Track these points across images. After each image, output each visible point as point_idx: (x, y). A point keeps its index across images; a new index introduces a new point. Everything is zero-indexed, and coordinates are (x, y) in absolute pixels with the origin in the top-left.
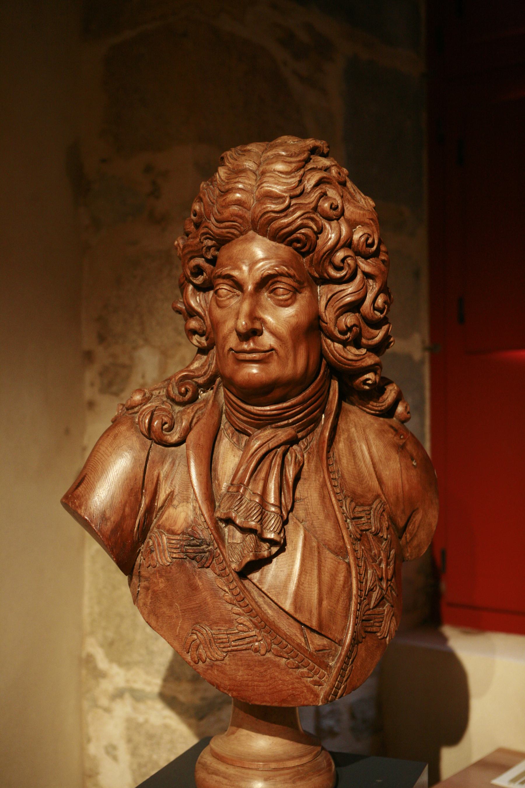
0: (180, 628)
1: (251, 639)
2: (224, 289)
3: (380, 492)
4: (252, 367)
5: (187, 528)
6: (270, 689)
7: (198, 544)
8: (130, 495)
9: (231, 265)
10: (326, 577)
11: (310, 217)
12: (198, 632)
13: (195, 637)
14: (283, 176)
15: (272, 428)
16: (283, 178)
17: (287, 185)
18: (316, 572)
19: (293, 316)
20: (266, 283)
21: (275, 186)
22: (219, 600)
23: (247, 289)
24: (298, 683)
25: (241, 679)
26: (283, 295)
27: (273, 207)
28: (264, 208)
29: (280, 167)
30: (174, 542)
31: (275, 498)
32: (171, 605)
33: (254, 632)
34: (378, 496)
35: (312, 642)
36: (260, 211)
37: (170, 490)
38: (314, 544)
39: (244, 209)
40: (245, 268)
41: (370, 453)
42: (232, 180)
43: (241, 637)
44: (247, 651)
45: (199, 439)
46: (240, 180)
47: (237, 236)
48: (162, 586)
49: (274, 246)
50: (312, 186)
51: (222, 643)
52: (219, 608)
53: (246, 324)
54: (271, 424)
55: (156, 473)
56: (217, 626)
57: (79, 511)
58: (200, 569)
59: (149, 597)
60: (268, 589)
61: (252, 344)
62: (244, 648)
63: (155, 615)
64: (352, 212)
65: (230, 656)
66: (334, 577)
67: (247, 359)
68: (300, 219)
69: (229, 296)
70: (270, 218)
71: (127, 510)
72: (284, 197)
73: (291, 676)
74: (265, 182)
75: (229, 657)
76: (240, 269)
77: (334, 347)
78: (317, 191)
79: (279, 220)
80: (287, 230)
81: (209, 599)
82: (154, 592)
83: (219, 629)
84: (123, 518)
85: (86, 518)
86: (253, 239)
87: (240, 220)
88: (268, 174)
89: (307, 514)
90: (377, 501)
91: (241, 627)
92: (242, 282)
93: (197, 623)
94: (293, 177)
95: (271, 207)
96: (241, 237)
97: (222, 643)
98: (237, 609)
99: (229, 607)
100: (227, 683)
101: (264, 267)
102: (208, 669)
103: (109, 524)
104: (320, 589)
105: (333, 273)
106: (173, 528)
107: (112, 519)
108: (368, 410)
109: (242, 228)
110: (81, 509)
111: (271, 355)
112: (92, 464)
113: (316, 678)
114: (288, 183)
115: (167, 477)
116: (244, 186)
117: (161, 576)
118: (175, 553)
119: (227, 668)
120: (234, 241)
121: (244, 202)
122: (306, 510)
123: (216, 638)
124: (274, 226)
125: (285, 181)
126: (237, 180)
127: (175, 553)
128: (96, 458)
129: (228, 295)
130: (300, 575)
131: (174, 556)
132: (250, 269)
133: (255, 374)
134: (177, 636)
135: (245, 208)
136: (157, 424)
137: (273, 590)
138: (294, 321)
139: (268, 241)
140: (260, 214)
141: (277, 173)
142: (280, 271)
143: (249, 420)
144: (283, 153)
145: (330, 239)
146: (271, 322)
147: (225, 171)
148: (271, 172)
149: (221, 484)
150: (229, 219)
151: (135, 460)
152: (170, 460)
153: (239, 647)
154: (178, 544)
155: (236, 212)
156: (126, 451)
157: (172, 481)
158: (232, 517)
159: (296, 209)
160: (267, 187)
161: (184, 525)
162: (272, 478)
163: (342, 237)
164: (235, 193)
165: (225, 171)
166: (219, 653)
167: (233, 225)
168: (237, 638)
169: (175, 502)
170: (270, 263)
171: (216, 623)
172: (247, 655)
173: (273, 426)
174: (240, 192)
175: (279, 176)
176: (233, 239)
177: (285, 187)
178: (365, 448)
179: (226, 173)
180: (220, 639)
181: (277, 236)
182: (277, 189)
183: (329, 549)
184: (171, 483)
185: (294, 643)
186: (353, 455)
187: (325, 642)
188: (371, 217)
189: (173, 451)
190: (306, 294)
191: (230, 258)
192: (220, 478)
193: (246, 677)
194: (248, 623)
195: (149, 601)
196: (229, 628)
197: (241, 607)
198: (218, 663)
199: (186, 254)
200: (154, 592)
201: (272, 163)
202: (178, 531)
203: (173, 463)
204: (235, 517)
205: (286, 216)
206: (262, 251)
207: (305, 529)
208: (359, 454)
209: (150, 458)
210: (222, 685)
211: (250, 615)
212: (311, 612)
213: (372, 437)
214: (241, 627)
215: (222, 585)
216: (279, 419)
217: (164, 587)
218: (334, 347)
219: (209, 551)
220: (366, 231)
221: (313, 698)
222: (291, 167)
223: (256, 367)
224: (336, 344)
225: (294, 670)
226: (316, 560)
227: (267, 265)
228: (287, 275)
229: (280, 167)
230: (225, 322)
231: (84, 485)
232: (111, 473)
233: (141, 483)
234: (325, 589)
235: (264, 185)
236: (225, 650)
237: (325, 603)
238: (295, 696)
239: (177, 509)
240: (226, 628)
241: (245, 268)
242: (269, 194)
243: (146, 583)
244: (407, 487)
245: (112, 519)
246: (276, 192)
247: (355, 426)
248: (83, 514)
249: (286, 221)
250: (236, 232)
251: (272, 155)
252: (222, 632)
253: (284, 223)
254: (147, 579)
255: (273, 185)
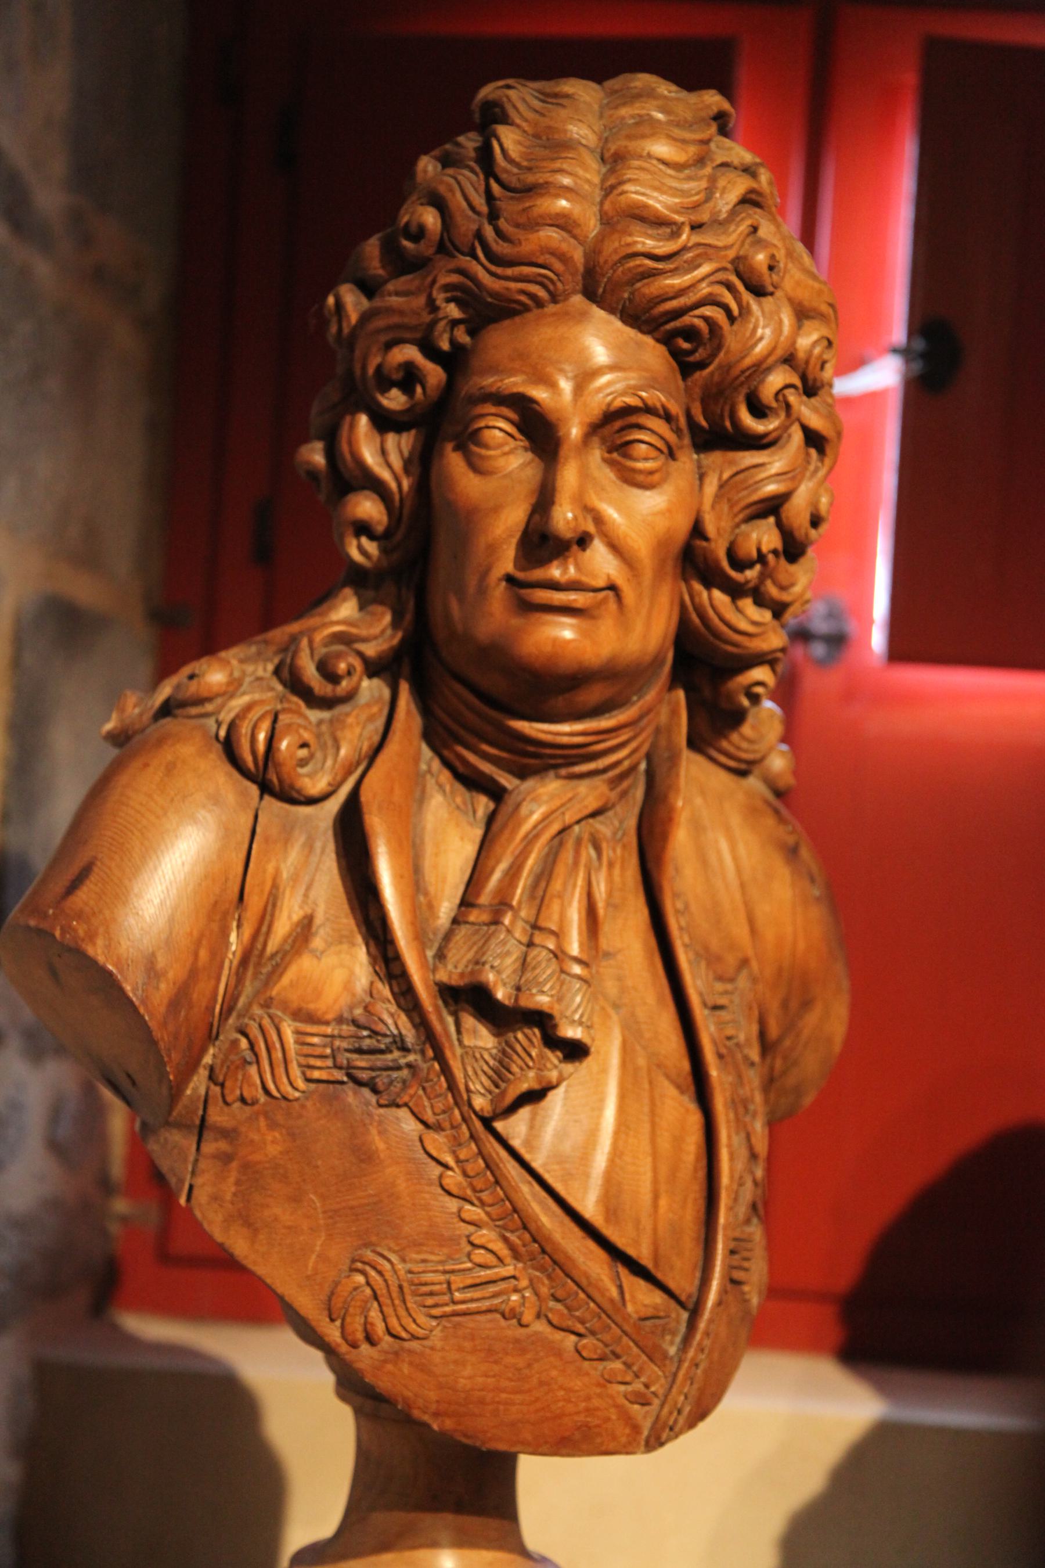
0: (318, 1256)
1: (502, 1286)
2: (498, 429)
3: (750, 953)
4: (563, 626)
5: (351, 1008)
6: (537, 1411)
7: (383, 1046)
8: (210, 918)
9: (524, 372)
10: (665, 1144)
11: (728, 280)
12: (368, 1268)
13: (360, 1279)
14: (670, 172)
15: (558, 777)
16: (671, 176)
17: (682, 196)
18: (646, 1127)
19: (661, 513)
20: (615, 427)
21: (655, 194)
22: (427, 1188)
23: (569, 433)
24: (600, 1396)
25: (468, 1387)
26: (646, 459)
27: (648, 244)
28: (629, 245)
29: (662, 149)
30: (316, 1040)
31: (581, 945)
32: (296, 1199)
33: (511, 1268)
34: (745, 962)
35: (633, 1297)
36: (615, 251)
37: (301, 913)
38: (641, 1062)
39: (572, 240)
40: (566, 386)
41: (735, 859)
42: (545, 164)
43: (478, 1281)
44: (489, 1316)
45: (392, 790)
46: (565, 166)
47: (539, 303)
48: (273, 1150)
49: (632, 339)
50: (730, 207)
51: (431, 1294)
52: (427, 1208)
53: (575, 518)
54: (555, 767)
55: (270, 868)
56: (418, 1253)
57: (90, 951)
58: (382, 1111)
59: (232, 1180)
60: (544, 1165)
61: (572, 570)
62: (484, 1308)
63: (247, 1223)
64: (798, 283)
65: (445, 1327)
66: (678, 1141)
67: (556, 603)
68: (707, 281)
69: (506, 449)
70: (641, 269)
71: (203, 954)
72: (675, 223)
73: (586, 1379)
74: (630, 180)
75: (442, 1331)
76: (553, 385)
77: (710, 598)
78: (743, 219)
79: (661, 278)
80: (674, 304)
81: (402, 1185)
82: (246, 1166)
83: (424, 1261)
84: (193, 974)
85: (110, 967)
86: (582, 316)
87: (558, 266)
88: (636, 163)
89: (623, 990)
90: (745, 973)
91: (480, 1256)
92: (553, 417)
93: (366, 1245)
94: (689, 178)
95: (644, 243)
96: (551, 308)
97: (431, 1294)
98: (473, 1212)
99: (453, 1205)
100: (433, 1395)
101: (611, 388)
102: (385, 1361)
103: (163, 986)
104: (655, 1170)
105: (747, 420)
106: (312, 1006)
107: (171, 975)
108: (723, 759)
109: (559, 285)
110: (94, 944)
111: (605, 600)
112: (109, 833)
113: (638, 1386)
114: (682, 191)
115: (295, 878)
116: (576, 184)
117: (273, 1125)
118: (319, 1068)
119: (437, 1358)
120: (529, 316)
121: (575, 222)
122: (620, 979)
123: (416, 1281)
124: (646, 291)
125: (675, 184)
126: (557, 165)
127: (319, 1068)
128: (119, 820)
129: (506, 444)
130: (617, 1133)
131: (316, 1074)
132: (579, 389)
133: (569, 642)
134: (308, 1277)
135: (575, 237)
136: (288, 746)
137: (556, 1167)
138: (662, 525)
139: (619, 324)
140: (616, 258)
141: (655, 162)
142: (650, 403)
143: (504, 755)
144: (660, 116)
145: (761, 339)
146: (614, 520)
147: (517, 137)
148: (640, 157)
149: (435, 904)
150: (534, 260)
151: (227, 832)
152: (302, 839)
153: (473, 1306)
154: (325, 1046)
155: (554, 244)
156: (204, 807)
157: (308, 888)
158: (488, 982)
159: (698, 256)
160: (636, 193)
161: (344, 1001)
162: (573, 894)
163: (782, 339)
164: (558, 196)
165: (517, 137)
166: (422, 1319)
167: (540, 275)
168: (469, 1282)
169: (317, 943)
170: (626, 379)
171: (417, 1245)
172: (488, 1326)
173: (563, 772)
174: (568, 195)
175: (660, 170)
176: (527, 309)
177: (677, 200)
178: (724, 846)
179: (520, 143)
180: (426, 1284)
181: (640, 316)
182: (659, 202)
183: (668, 1077)
184: (306, 895)
185: (603, 1295)
186: (704, 861)
187: (657, 1298)
188: (830, 301)
189: (308, 818)
190: (684, 463)
191: (522, 356)
192: (432, 890)
193: (480, 1380)
194: (499, 1247)
195: (229, 1189)
196: (450, 1257)
197: (483, 1204)
198: (414, 1345)
199: (378, 331)
200: (246, 1166)
201: (643, 136)
202: (325, 1013)
203: (309, 846)
204: (495, 984)
205: (674, 272)
206: (606, 347)
207: (625, 1027)
208: (713, 859)
209: (258, 830)
210: (420, 1402)
211: (504, 1227)
212: (637, 1222)
213: (735, 820)
214: (480, 1256)
215: (439, 1150)
216: (575, 756)
217: (281, 1153)
218: (710, 598)
219: (409, 1066)
220: (825, 331)
221: (628, 1435)
222: (686, 152)
223: (572, 626)
224: (717, 594)
225: (595, 1363)
226: (646, 1101)
227: (619, 381)
228: (661, 412)
229: (662, 149)
230: (497, 509)
231: (92, 886)
232: (167, 859)
233: (236, 889)
234: (664, 1170)
235: (629, 187)
236: (436, 1312)
237: (663, 1202)
238: (590, 1428)
239: (324, 960)
240: (442, 1258)
241: (566, 386)
242: (637, 211)
243: (223, 1145)
244: (801, 945)
245: (171, 975)
246: (657, 210)
247: (703, 793)
248: (101, 959)
249: (676, 282)
250: (542, 293)
251: (632, 117)
252: (430, 1266)
253: (672, 286)
254: (227, 1134)
255: (648, 192)
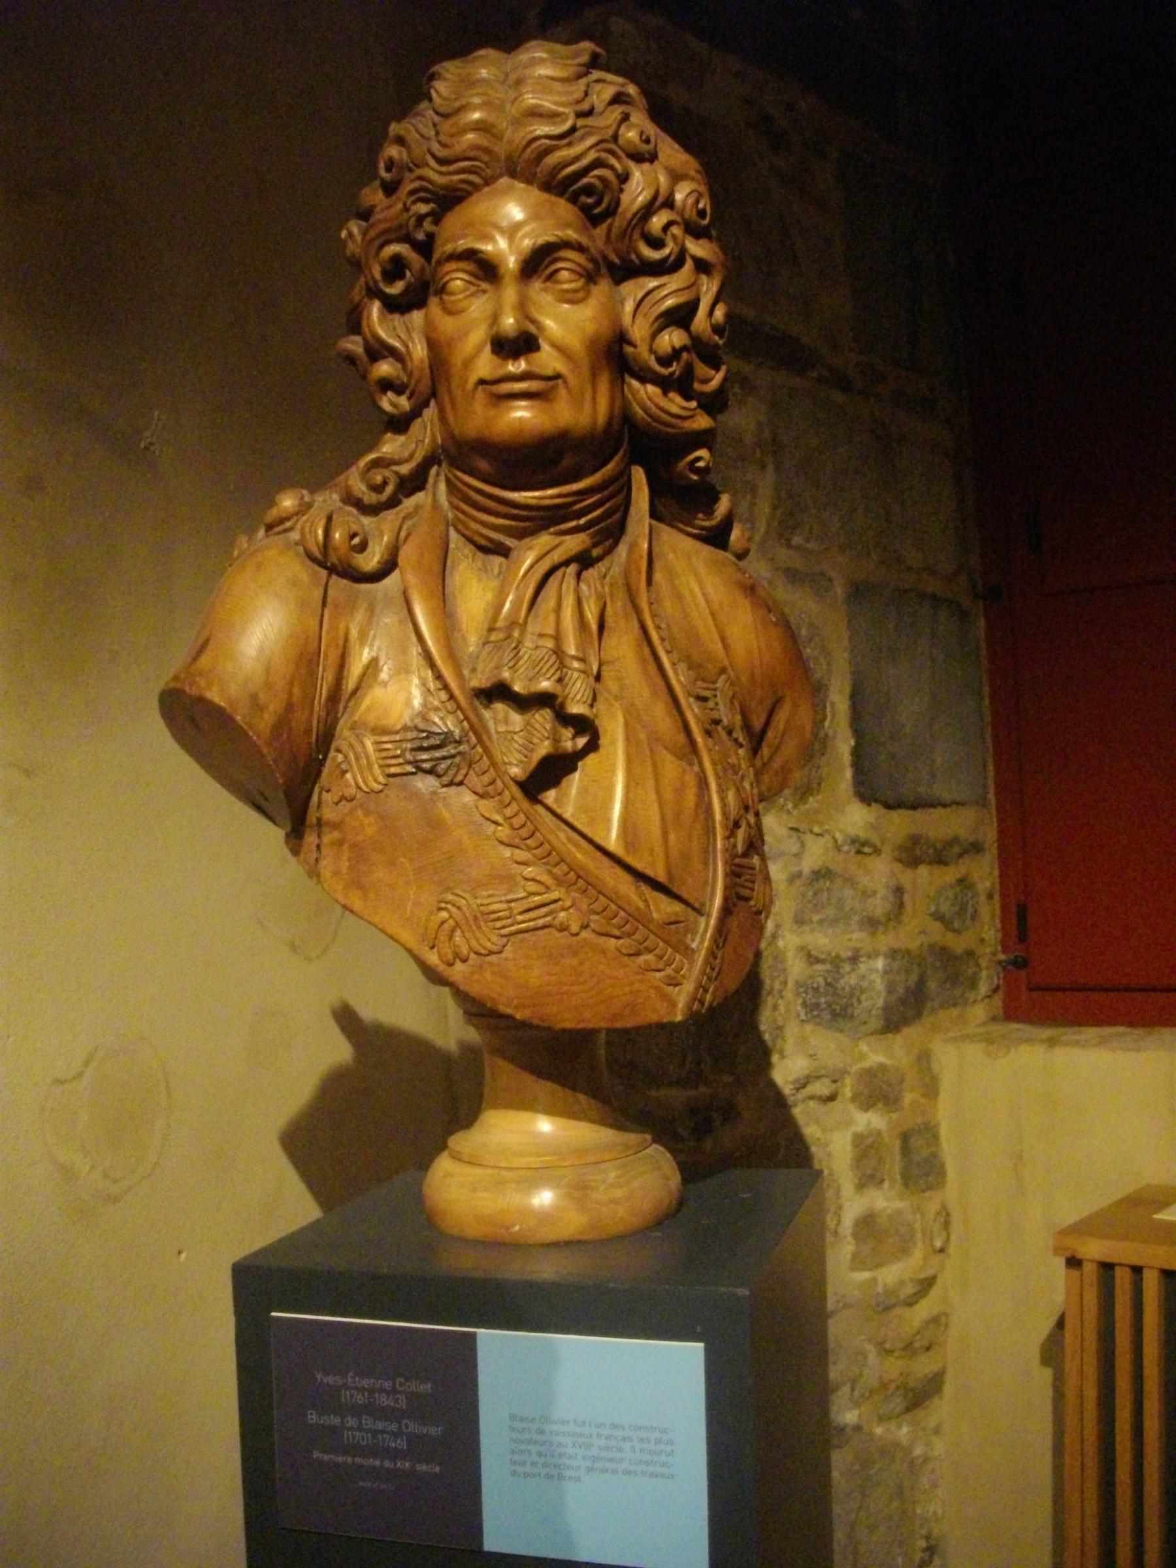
2: (458, 280)
3: (726, 663)
5: (412, 720)
10: (669, 795)
12: (449, 906)
13: (444, 914)
18: (651, 783)
24: (640, 981)
28: (531, 132)
30: (388, 746)
34: (723, 670)
38: (642, 736)
44: (546, 931)
47: (477, 188)
48: (370, 831)
51: (498, 919)
58: (444, 790)
66: (680, 791)
77: (646, 393)
82: (353, 846)
84: (290, 707)
87: (486, 158)
91: (532, 887)
93: (448, 889)
96: (486, 189)
97: (498, 919)
99: (507, 852)
103: (266, 716)
106: (384, 722)
107: (271, 707)
113: (669, 971)
117: (367, 813)
119: (510, 965)
131: (393, 770)
138: (590, 328)
140: (524, 143)
152: (365, 605)
168: (525, 907)
169: (384, 676)
176: (469, 194)
180: (494, 912)
183: (666, 748)
185: (630, 905)
186: (679, 596)
187: (678, 907)
194: (544, 878)
195: (344, 865)
197: (529, 849)
198: (493, 958)
199: (374, 239)
204: (512, 679)
205: (570, 144)
208: (687, 594)
211: (547, 863)
212: (652, 852)
213: (702, 570)
218: (646, 393)
226: (649, 763)
230: (466, 334)
233: (316, 644)
234: (669, 815)
236: (506, 931)
237: (672, 837)
243: (336, 835)
245: (271, 707)
254: (335, 826)
